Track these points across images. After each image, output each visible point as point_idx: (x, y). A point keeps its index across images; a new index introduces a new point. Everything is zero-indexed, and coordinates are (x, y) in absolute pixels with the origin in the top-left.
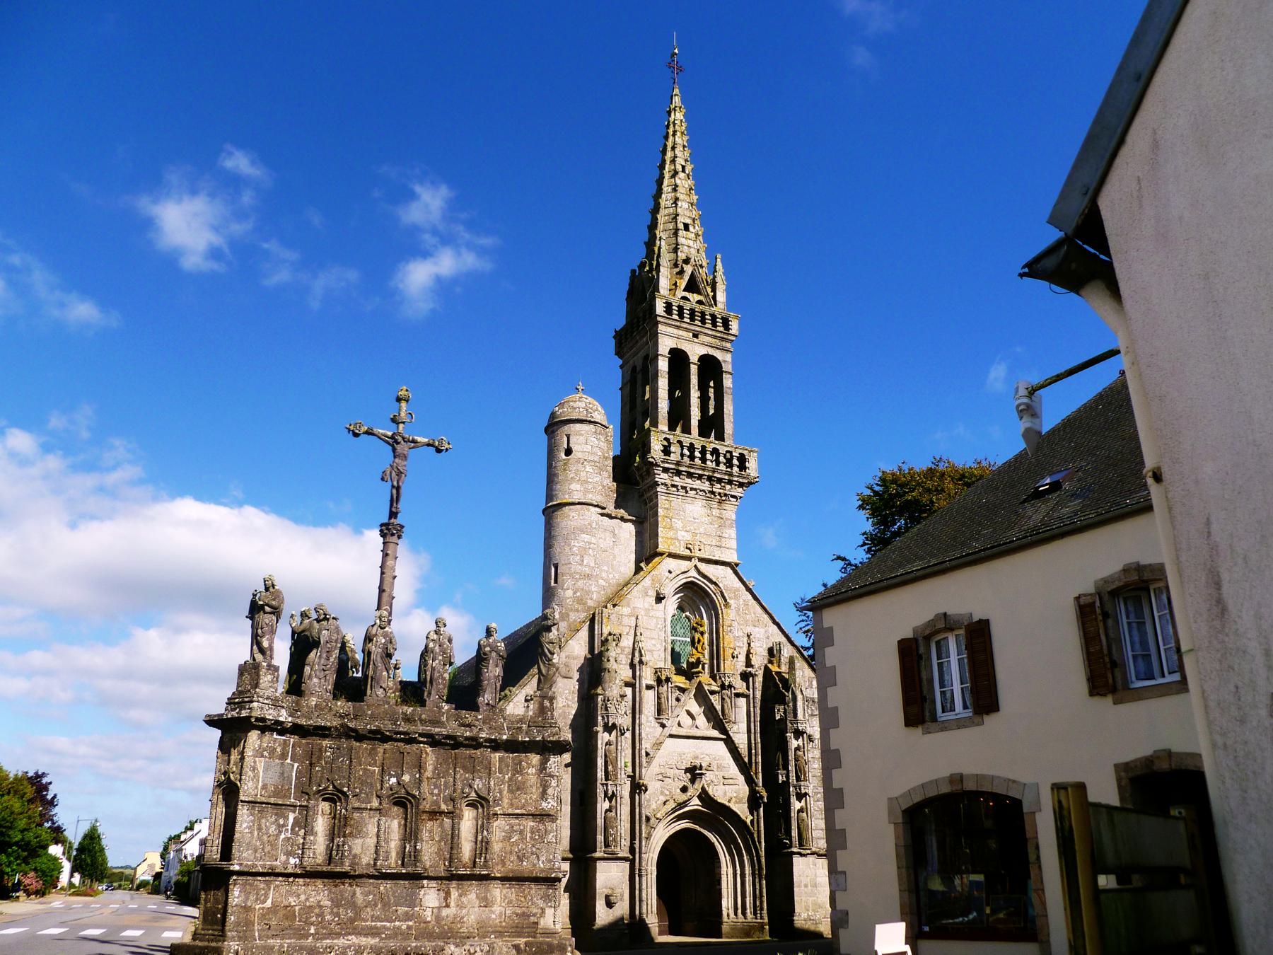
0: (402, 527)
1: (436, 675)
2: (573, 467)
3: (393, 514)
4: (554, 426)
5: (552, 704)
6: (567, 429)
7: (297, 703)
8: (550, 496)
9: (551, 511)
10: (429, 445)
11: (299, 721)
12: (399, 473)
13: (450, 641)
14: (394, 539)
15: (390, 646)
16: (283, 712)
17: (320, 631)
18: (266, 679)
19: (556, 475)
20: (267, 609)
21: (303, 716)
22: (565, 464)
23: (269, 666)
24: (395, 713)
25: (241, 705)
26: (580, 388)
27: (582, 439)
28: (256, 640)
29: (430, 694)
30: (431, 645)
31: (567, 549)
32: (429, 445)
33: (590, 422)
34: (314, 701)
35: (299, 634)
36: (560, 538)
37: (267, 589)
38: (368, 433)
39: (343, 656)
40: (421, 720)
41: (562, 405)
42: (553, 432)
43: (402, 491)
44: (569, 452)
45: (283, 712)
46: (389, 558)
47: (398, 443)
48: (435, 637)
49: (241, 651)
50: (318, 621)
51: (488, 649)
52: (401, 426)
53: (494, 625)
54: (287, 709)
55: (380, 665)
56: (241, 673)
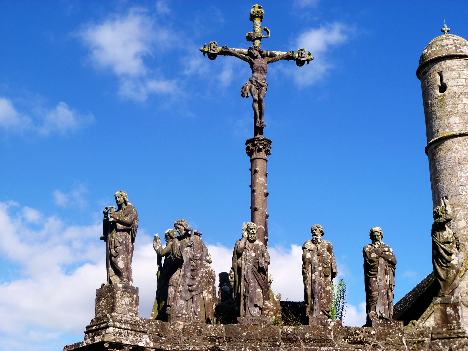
0: (270, 142)
1: (317, 288)
2: (449, 102)
3: (258, 130)
4: (425, 66)
5: (456, 311)
6: (438, 67)
7: (162, 328)
8: (430, 132)
9: (433, 147)
10: (288, 58)
11: (163, 347)
12: (259, 87)
13: (330, 250)
14: (262, 155)
15: (262, 260)
16: (146, 338)
17: (181, 248)
18: (123, 302)
19: (434, 112)
20: (119, 226)
21: (169, 341)
22: (441, 100)
23: (126, 288)
24: (274, 333)
25: (97, 332)
26: (446, 29)
27: (455, 74)
28: (111, 261)
29: (312, 309)
30: (308, 255)
31: (455, 180)
32: (288, 58)
33: (460, 57)
34: (180, 325)
35: (167, 255)
36: (446, 171)
37: (120, 207)
38: (225, 53)
39: (226, 288)
40: (304, 340)
41: (430, 46)
42: (425, 73)
43: (264, 104)
44: (443, 88)
45: (146, 338)
46: (258, 175)
47: (255, 57)
48: (312, 246)
49: (96, 275)
50: (180, 238)
51: (374, 255)
52: (257, 42)
53: (378, 229)
54: (151, 334)
55: (253, 282)
56: (98, 300)
